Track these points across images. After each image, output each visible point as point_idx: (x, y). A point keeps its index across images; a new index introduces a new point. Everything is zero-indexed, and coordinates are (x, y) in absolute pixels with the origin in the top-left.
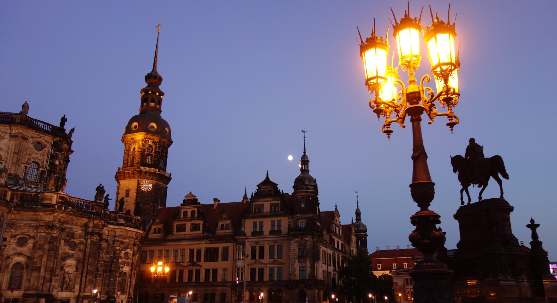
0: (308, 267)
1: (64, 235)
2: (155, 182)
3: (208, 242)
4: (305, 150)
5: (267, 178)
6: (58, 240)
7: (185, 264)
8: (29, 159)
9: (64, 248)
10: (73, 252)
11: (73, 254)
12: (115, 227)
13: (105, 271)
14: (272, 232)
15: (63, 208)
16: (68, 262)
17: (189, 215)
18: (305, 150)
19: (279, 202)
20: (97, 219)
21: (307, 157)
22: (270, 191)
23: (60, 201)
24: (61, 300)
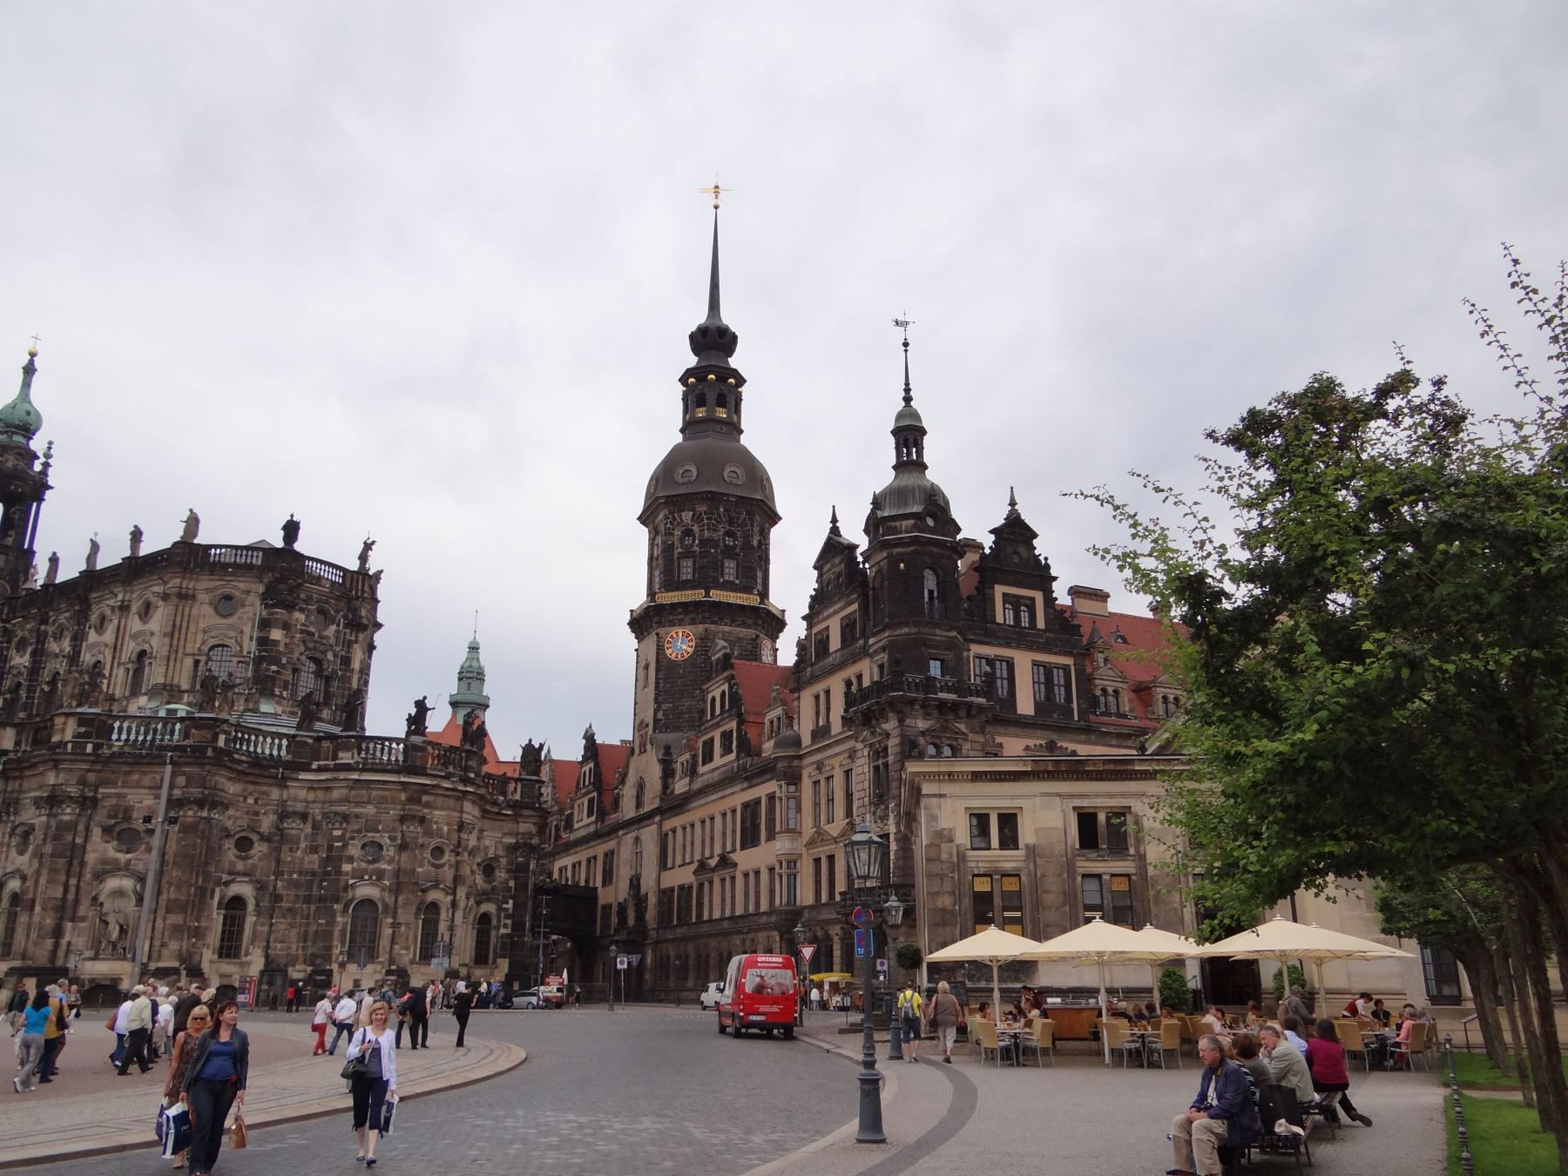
0: (892, 837)
1: (101, 816)
2: (701, 627)
3: (745, 785)
4: (907, 390)
5: (835, 530)
6: (81, 827)
7: (713, 863)
8: (203, 643)
9: (100, 849)
10: (129, 856)
11: (129, 861)
12: (323, 776)
13: (308, 900)
14: (846, 721)
15: (89, 748)
16: (112, 883)
17: (718, 712)
18: (907, 390)
19: (855, 606)
20: (186, 764)
21: (916, 416)
22: (839, 576)
23: (82, 730)
24: (92, 981)
